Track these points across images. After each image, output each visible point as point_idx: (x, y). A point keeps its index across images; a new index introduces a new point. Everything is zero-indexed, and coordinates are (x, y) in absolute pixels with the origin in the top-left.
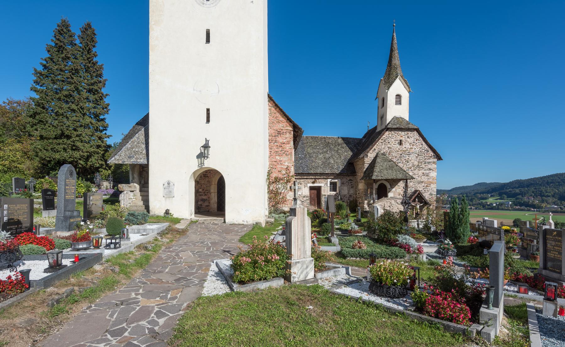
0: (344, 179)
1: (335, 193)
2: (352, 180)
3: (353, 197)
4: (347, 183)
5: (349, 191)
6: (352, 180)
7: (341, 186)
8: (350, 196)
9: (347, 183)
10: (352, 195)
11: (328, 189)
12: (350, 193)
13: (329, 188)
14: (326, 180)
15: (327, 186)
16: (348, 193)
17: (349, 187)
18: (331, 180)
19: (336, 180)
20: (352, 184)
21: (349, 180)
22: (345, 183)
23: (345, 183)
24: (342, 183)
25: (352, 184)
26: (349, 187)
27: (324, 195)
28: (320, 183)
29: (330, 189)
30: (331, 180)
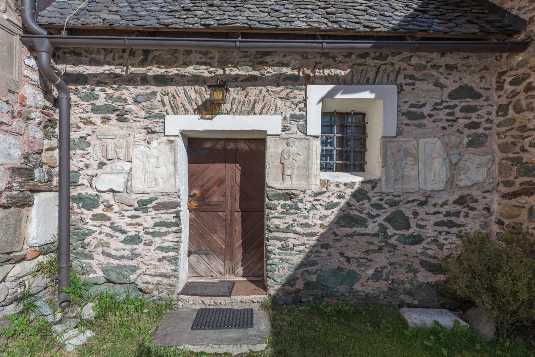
0: (419, 85)
1: (357, 179)
2: (478, 96)
3: (480, 206)
4: (442, 114)
5: (453, 167)
6: (478, 96)
7: (399, 133)
8: (461, 201)
9: (442, 114)
10: (476, 193)
11: (308, 149)
12: (465, 182)
13: (317, 145)
14: (298, 94)
15: (304, 130)
16: (450, 183)
17: (454, 139)
18: (329, 87)
19: (367, 95)
20: (474, 117)
21: (452, 96)
22: (426, 110)
23: (426, 110)
24: (409, 115)
25: (474, 117)
26: (454, 139)
27: (279, 197)
28: (252, 112)
29: (325, 155)
30: (330, 95)
